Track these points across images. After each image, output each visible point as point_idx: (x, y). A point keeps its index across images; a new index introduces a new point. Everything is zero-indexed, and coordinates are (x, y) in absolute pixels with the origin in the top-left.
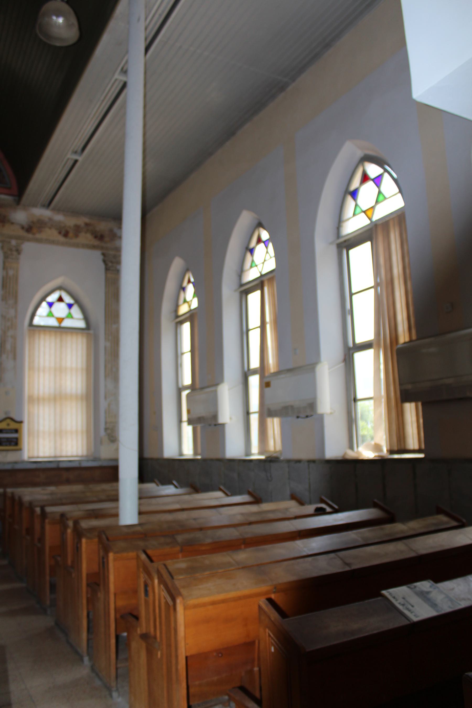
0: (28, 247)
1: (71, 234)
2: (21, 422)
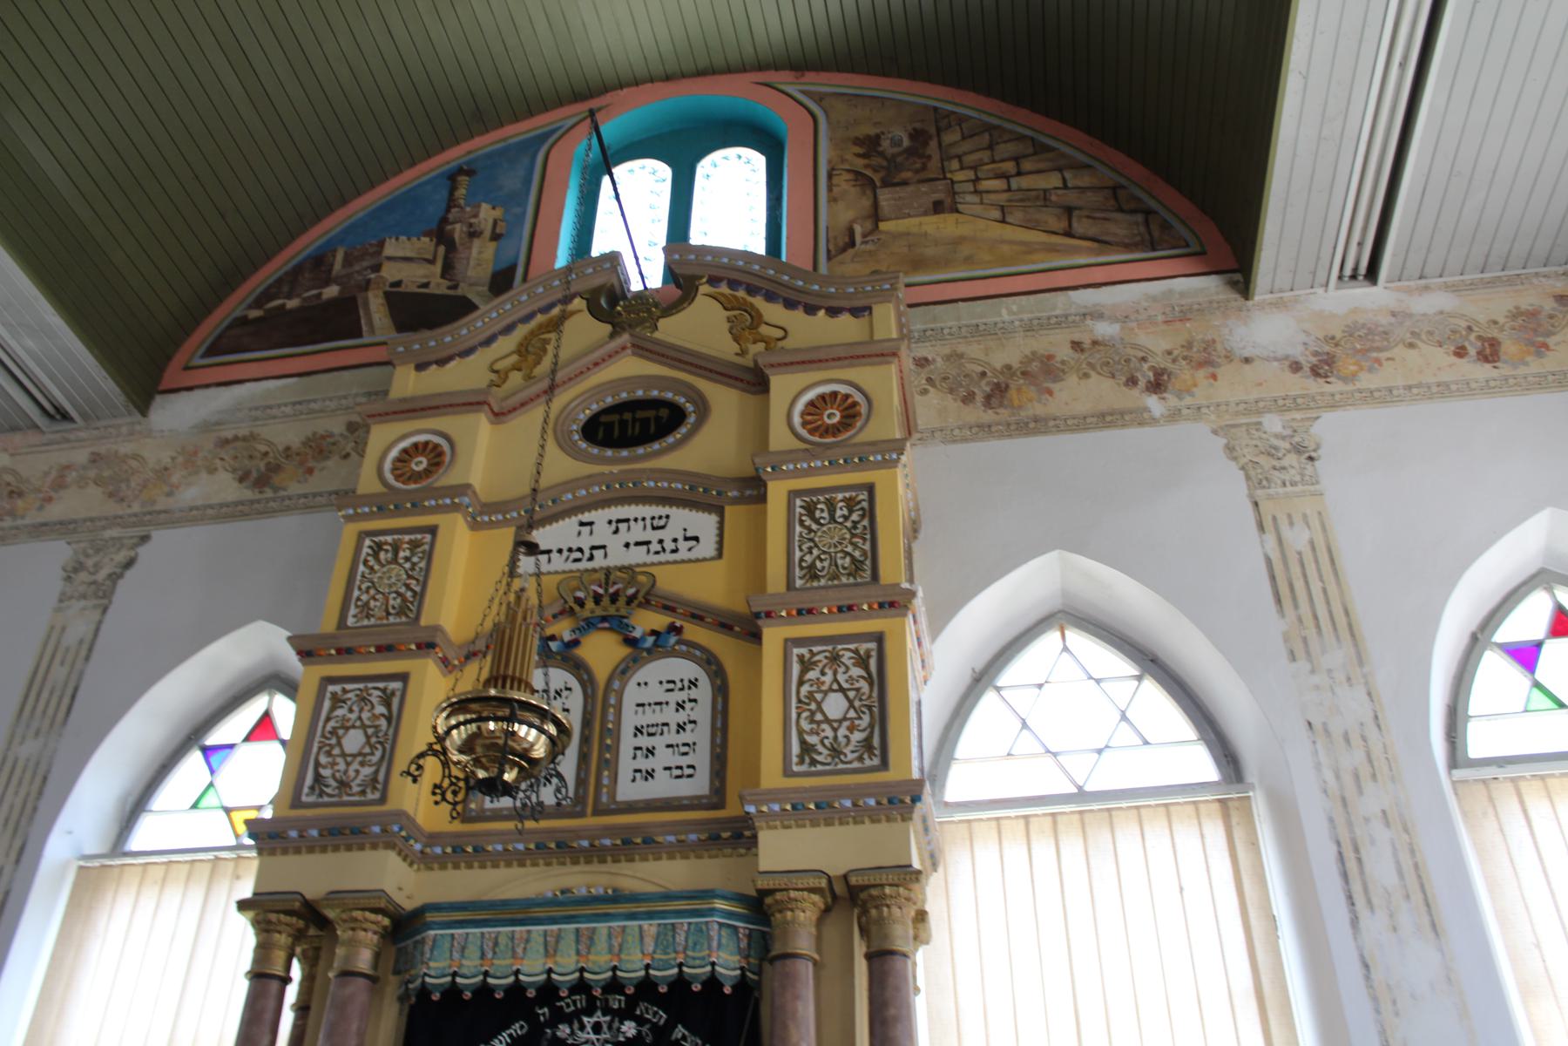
0: (1340, 430)
1: (1509, 347)
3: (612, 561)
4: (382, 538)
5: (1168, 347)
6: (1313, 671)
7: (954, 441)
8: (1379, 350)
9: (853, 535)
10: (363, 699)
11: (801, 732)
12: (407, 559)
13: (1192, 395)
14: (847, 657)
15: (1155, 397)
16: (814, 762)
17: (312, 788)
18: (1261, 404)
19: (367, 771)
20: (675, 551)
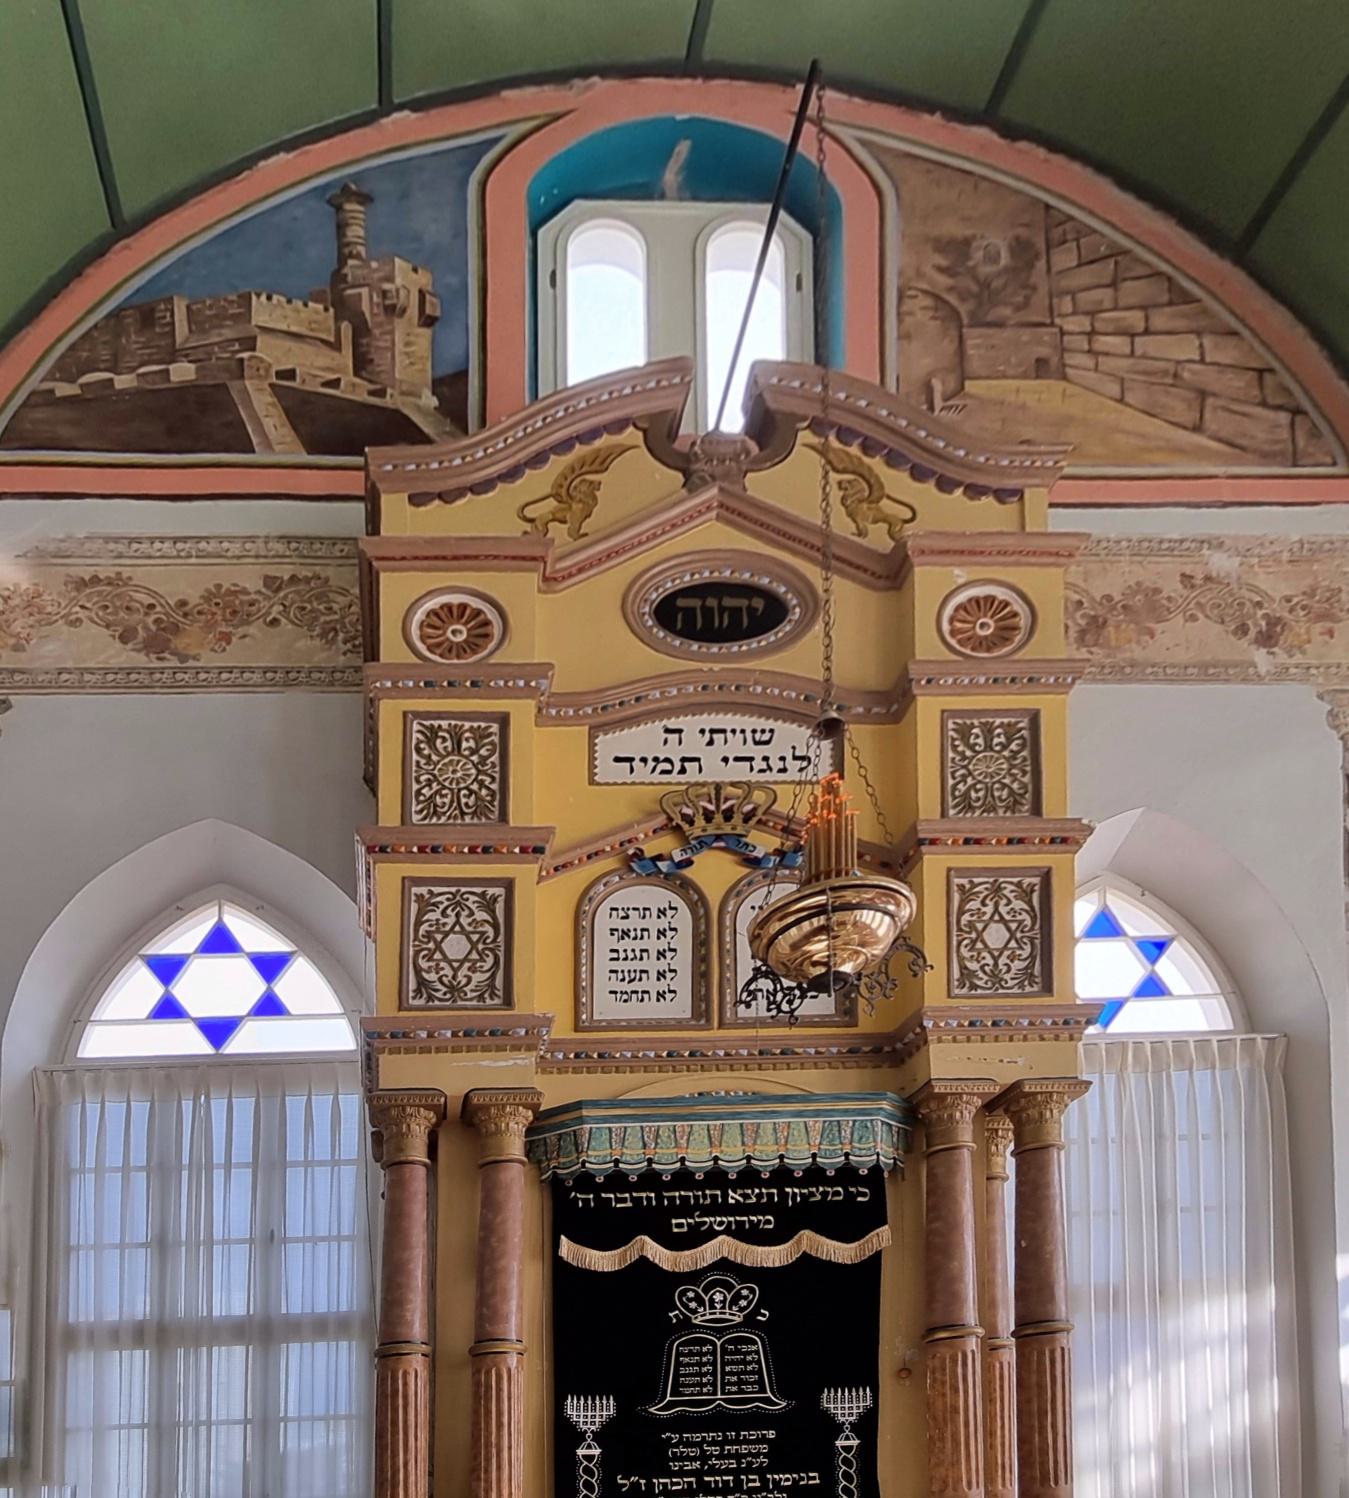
5: (1288, 593)
11: (961, 959)
14: (1008, 890)
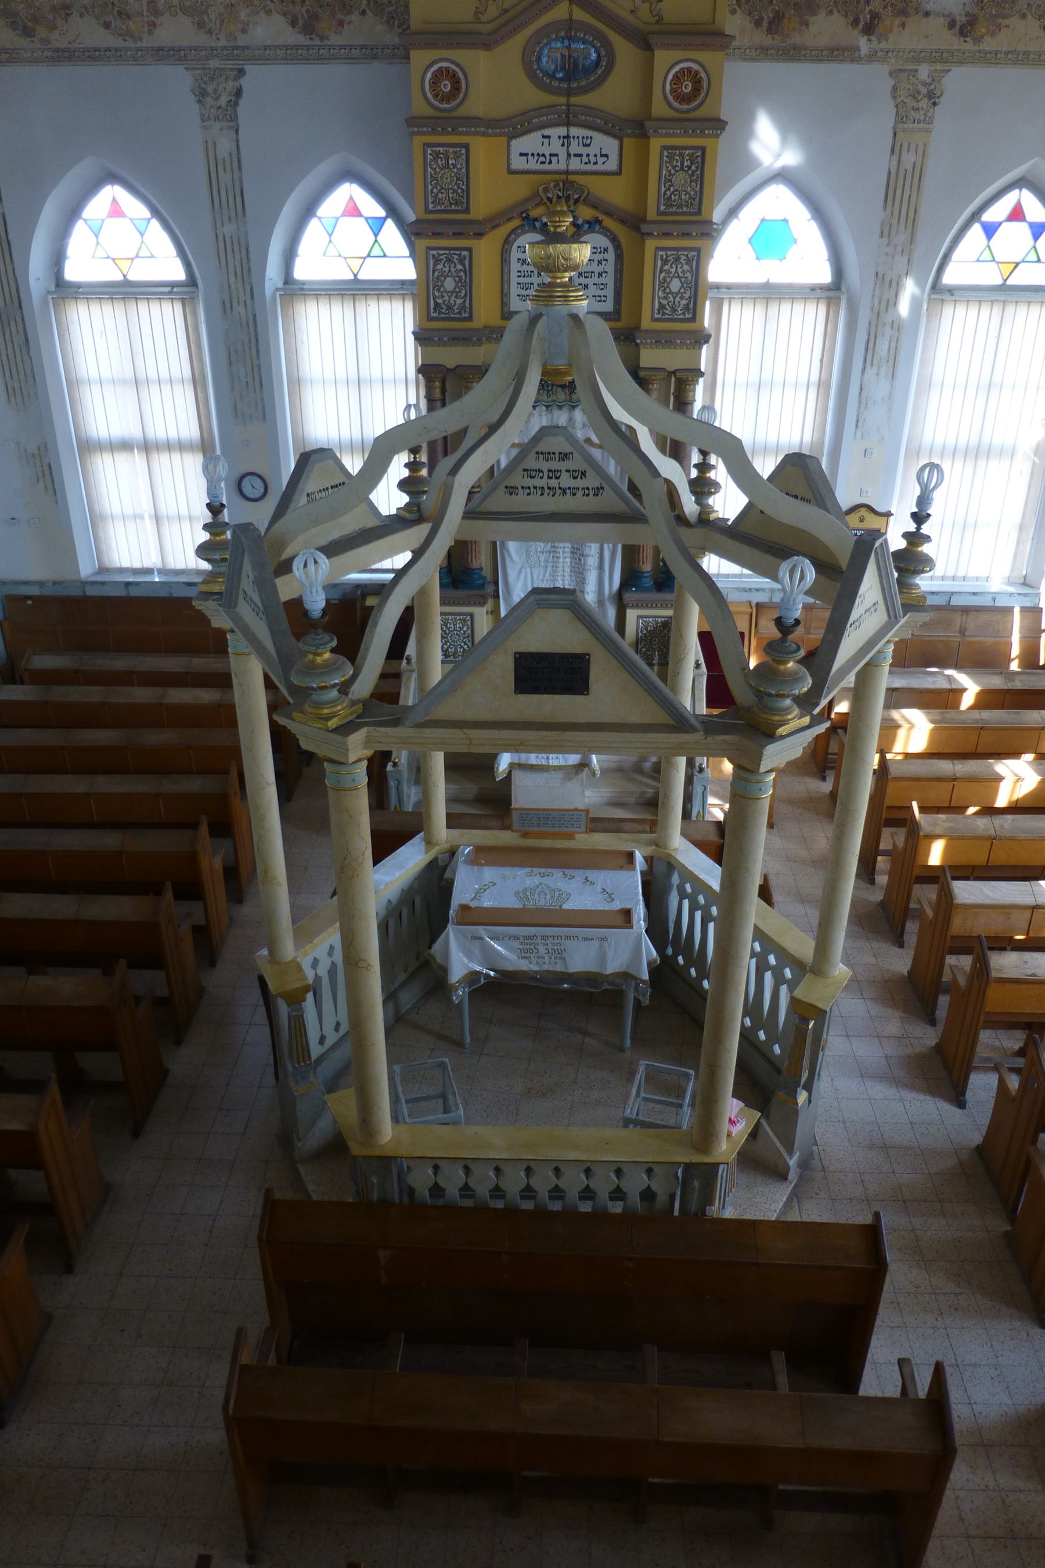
0: (958, 81)
2: (888, 514)
3: (562, 166)
4: (437, 149)
6: (888, 245)
7: (745, 60)
8: (1005, 17)
9: (691, 181)
10: (449, 260)
12: (454, 166)
13: (887, 40)
15: (866, 38)
16: (664, 314)
17: (435, 309)
18: (922, 55)
19: (459, 301)
20: (596, 163)
